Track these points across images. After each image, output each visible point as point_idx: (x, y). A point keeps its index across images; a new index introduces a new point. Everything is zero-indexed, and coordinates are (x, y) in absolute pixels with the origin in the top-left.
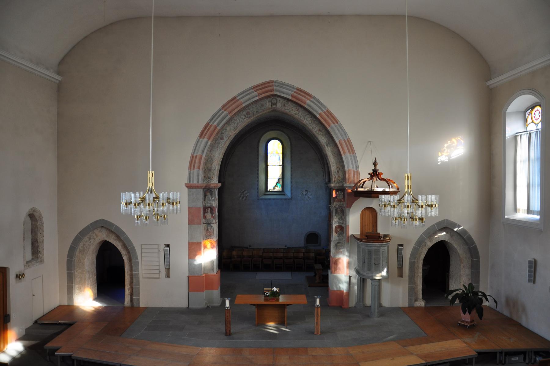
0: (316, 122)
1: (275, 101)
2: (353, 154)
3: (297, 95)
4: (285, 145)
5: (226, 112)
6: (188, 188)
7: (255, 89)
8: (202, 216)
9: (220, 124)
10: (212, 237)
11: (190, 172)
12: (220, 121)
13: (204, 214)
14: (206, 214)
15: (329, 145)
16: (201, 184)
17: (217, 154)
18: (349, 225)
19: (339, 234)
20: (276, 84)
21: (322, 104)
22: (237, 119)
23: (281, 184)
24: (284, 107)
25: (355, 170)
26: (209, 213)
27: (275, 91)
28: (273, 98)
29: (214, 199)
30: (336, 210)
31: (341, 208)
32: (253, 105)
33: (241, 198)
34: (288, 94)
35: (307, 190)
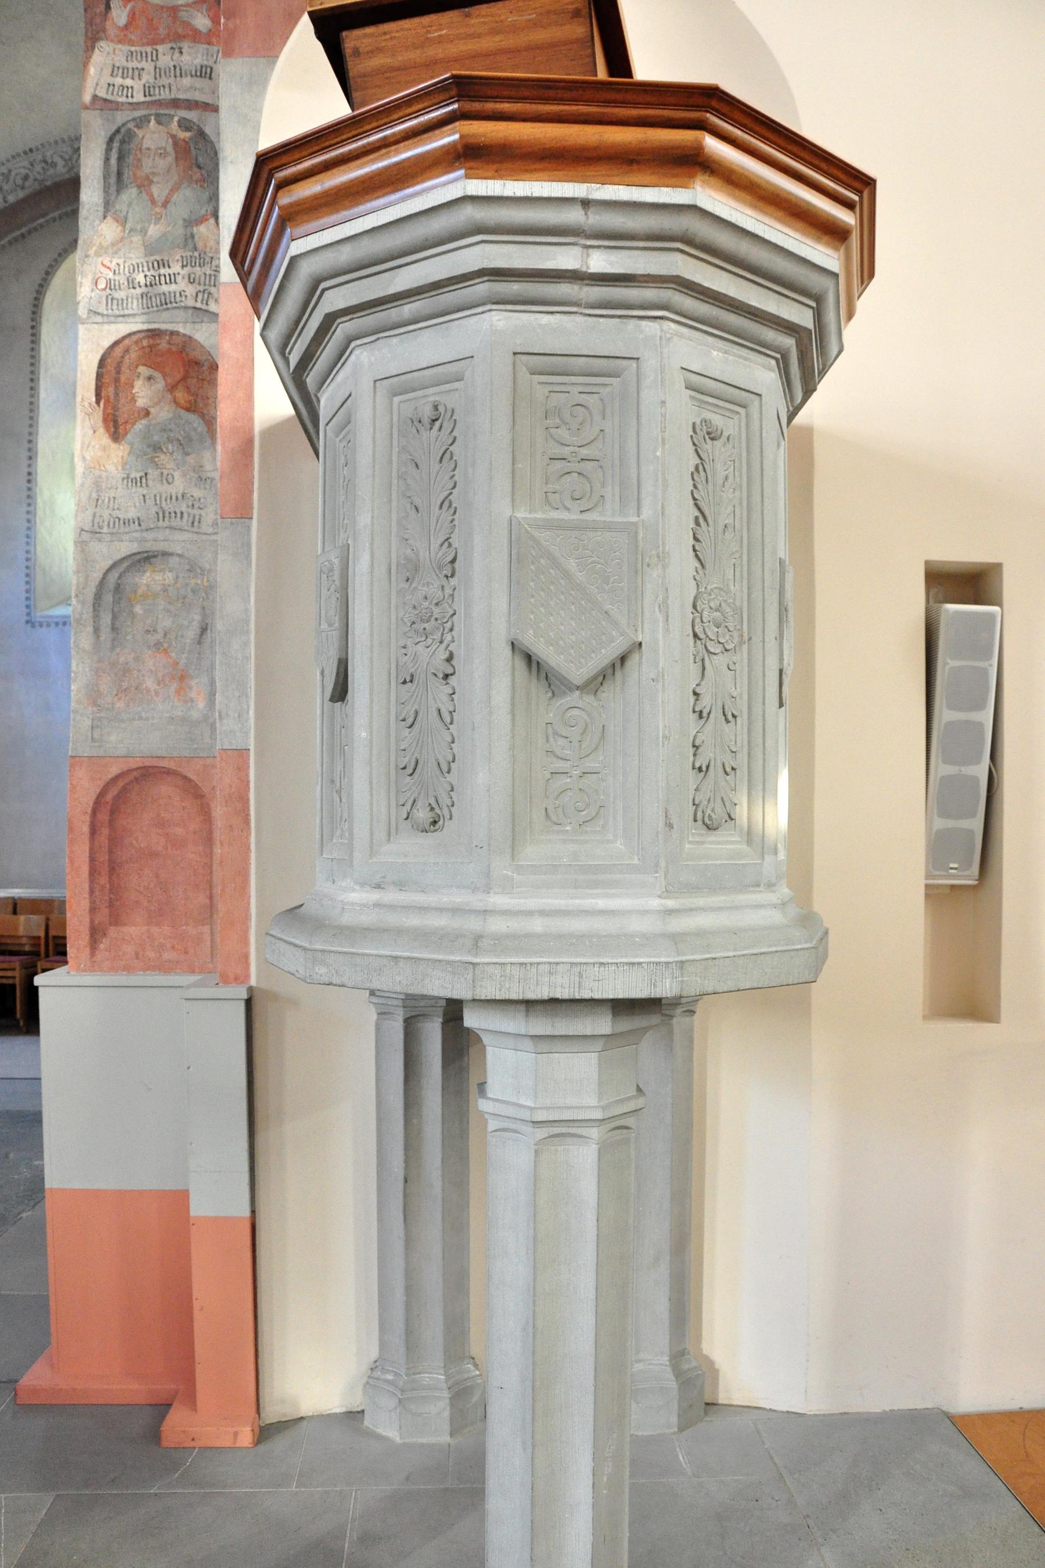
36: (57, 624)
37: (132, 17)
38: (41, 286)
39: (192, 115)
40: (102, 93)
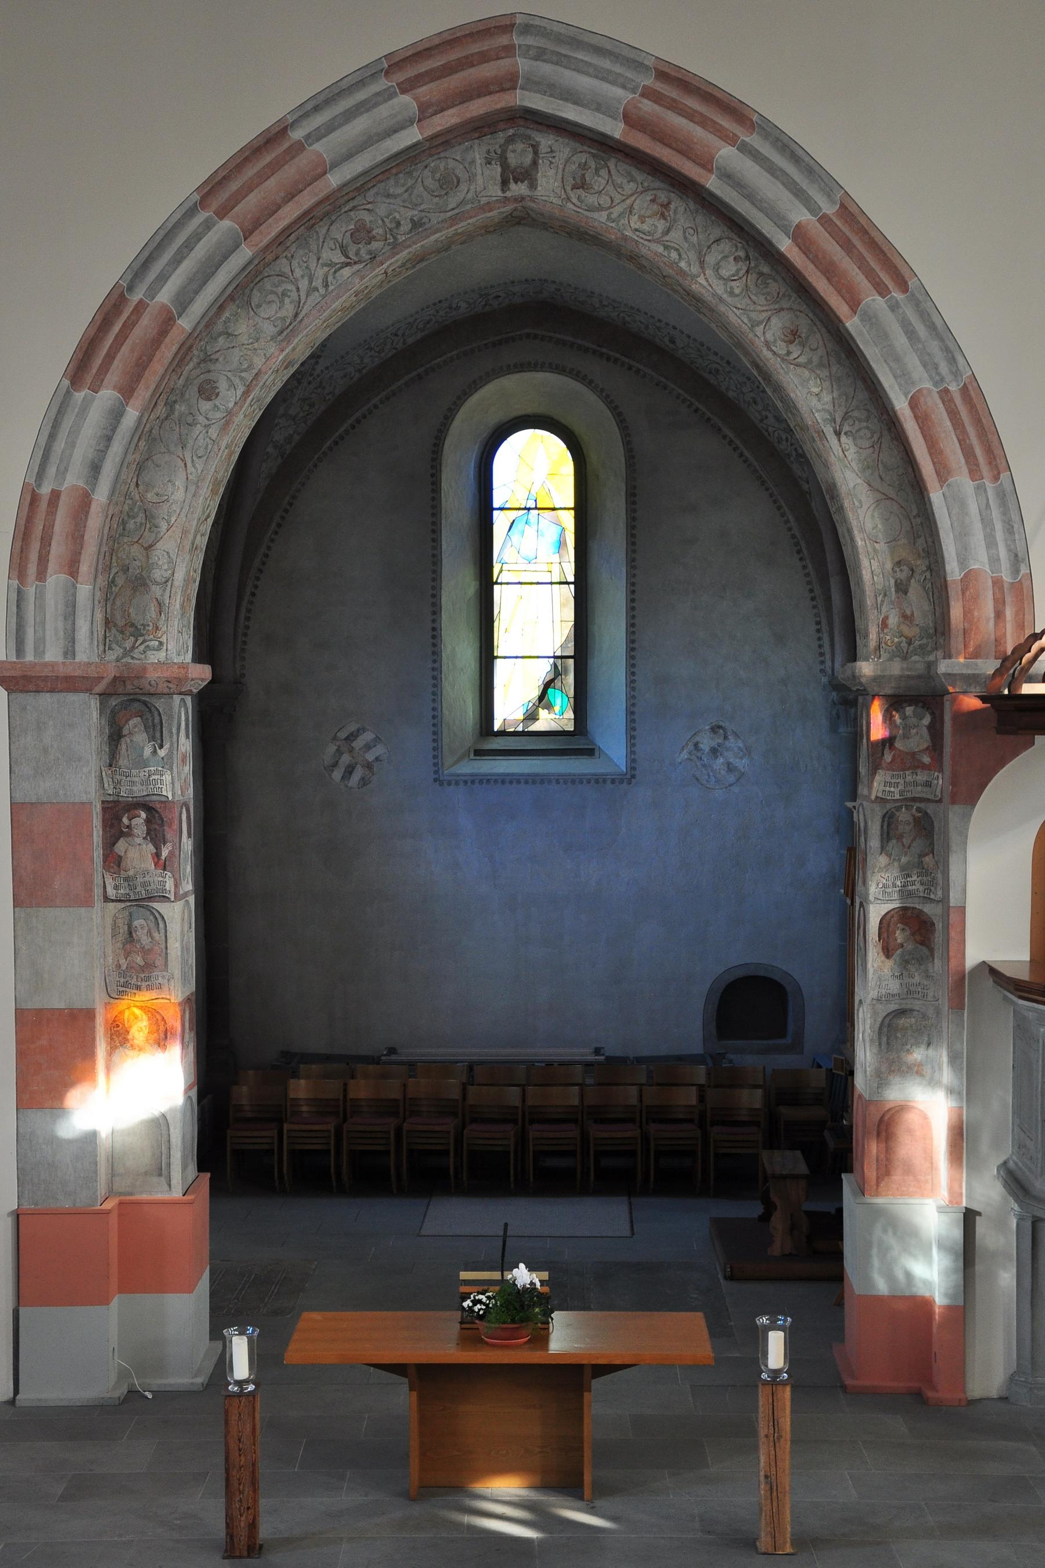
0: (774, 287)
1: (524, 151)
2: (996, 478)
3: (657, 108)
4: (593, 458)
5: (226, 224)
6: (9, 691)
7: (401, 76)
8: (98, 854)
9: (192, 300)
10: (160, 980)
11: (19, 592)
12: (191, 280)
13: (110, 844)
14: (121, 846)
15: (846, 428)
16: (89, 664)
17: (180, 482)
18: (962, 910)
19: (904, 963)
20: (530, 40)
21: (812, 170)
22: (298, 272)
23: (572, 693)
24: (580, 192)
25: (1007, 578)
26: (138, 840)
27: (522, 88)
28: (511, 132)
29: (171, 752)
30: (889, 821)
31: (918, 804)
32: (392, 182)
33: (337, 775)
34: (599, 106)
35: (720, 727)
36: (466, 782)
37: (894, 756)
38: (440, 431)
39: (922, 805)
40: (880, 795)
